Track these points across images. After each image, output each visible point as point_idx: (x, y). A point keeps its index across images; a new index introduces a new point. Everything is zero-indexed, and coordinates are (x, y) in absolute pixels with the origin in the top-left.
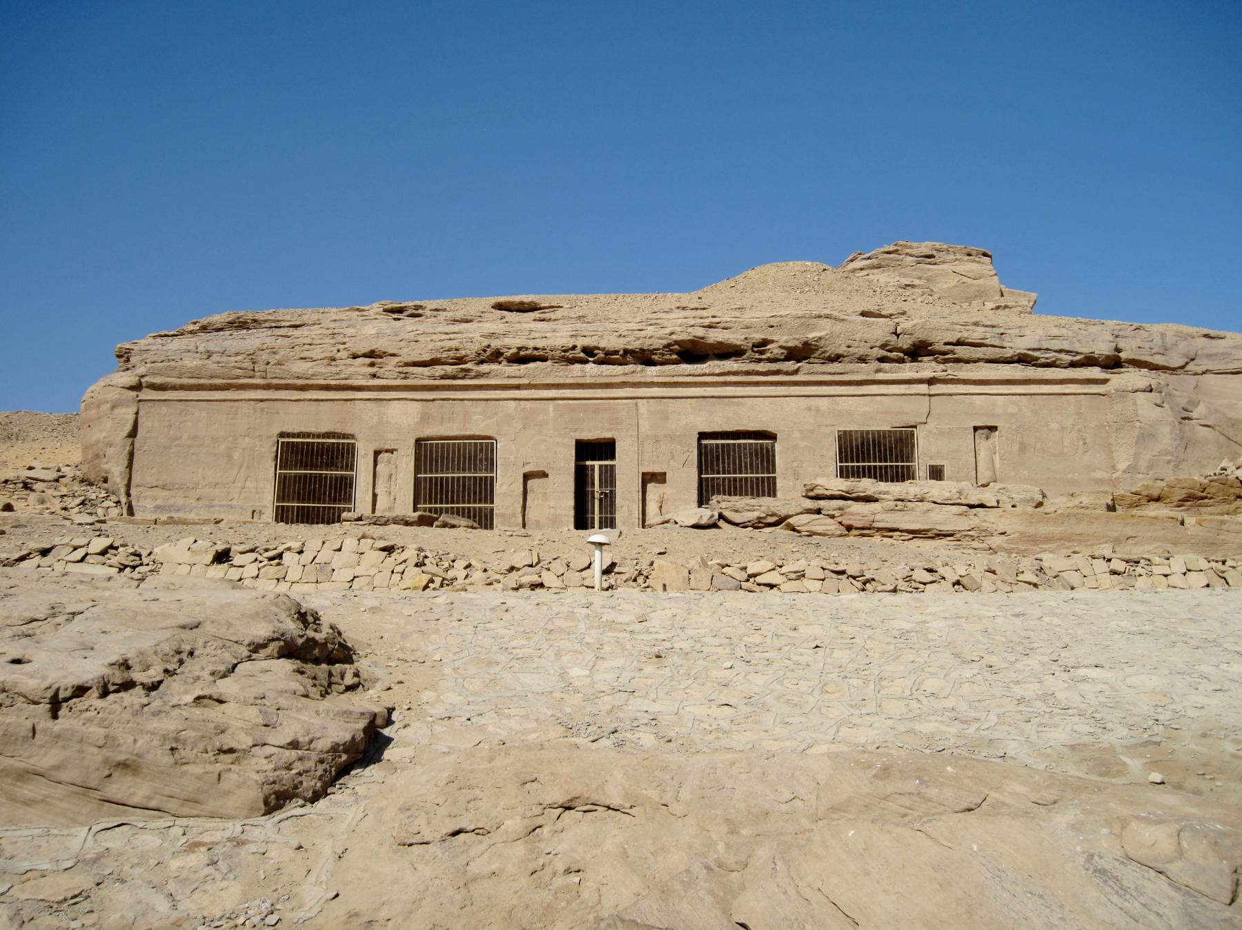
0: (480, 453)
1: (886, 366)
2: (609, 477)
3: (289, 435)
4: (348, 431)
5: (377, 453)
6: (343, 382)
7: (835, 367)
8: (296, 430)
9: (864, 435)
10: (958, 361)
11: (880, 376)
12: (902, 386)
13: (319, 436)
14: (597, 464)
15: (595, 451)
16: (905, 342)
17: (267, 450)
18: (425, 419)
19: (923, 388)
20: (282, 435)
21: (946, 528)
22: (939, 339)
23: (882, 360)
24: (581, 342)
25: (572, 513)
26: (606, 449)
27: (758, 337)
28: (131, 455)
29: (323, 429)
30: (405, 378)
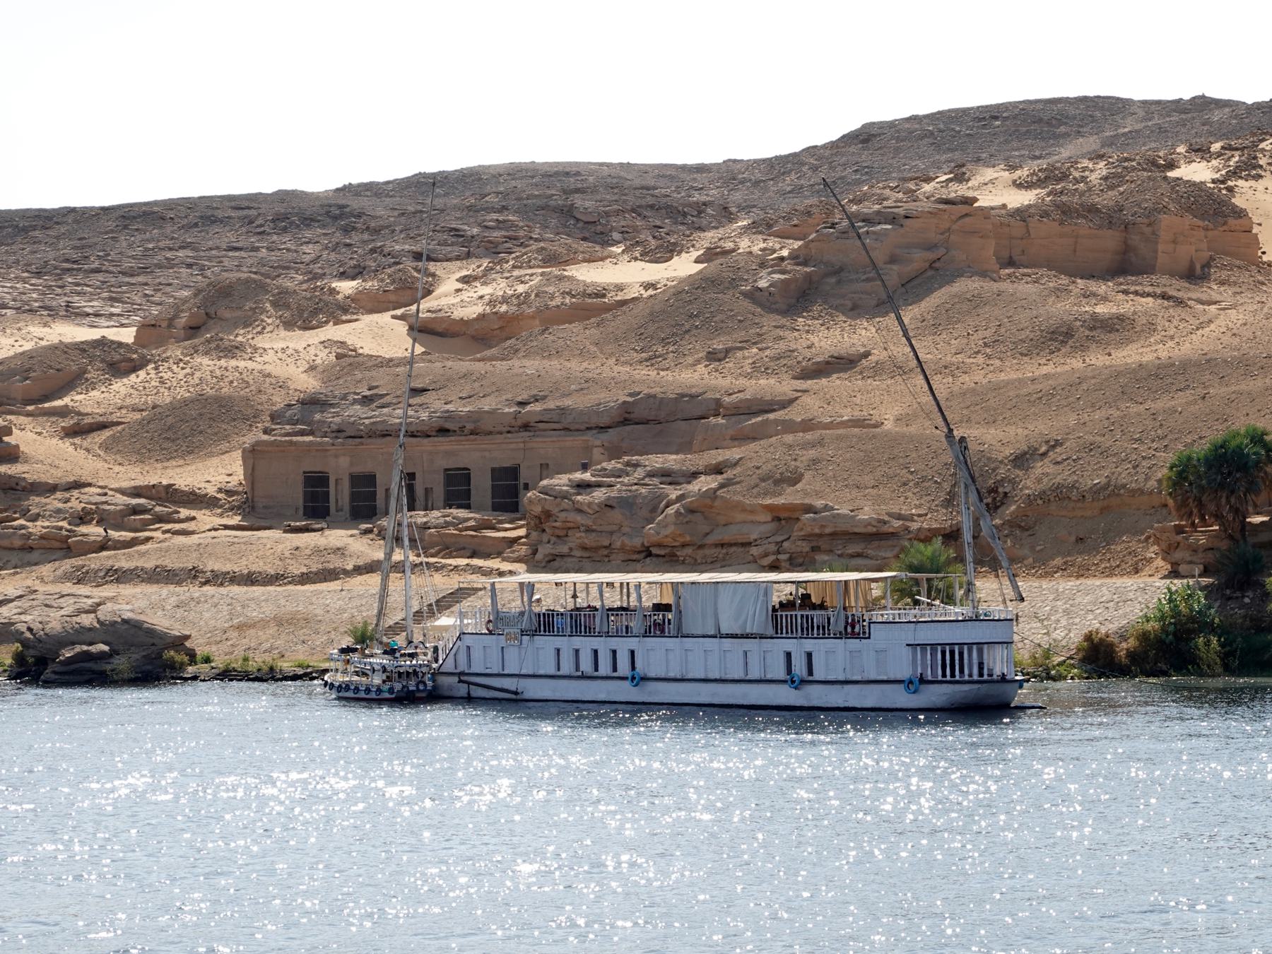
0: (370, 479)
16: (519, 423)
17: (301, 479)
19: (522, 445)
22: (533, 419)
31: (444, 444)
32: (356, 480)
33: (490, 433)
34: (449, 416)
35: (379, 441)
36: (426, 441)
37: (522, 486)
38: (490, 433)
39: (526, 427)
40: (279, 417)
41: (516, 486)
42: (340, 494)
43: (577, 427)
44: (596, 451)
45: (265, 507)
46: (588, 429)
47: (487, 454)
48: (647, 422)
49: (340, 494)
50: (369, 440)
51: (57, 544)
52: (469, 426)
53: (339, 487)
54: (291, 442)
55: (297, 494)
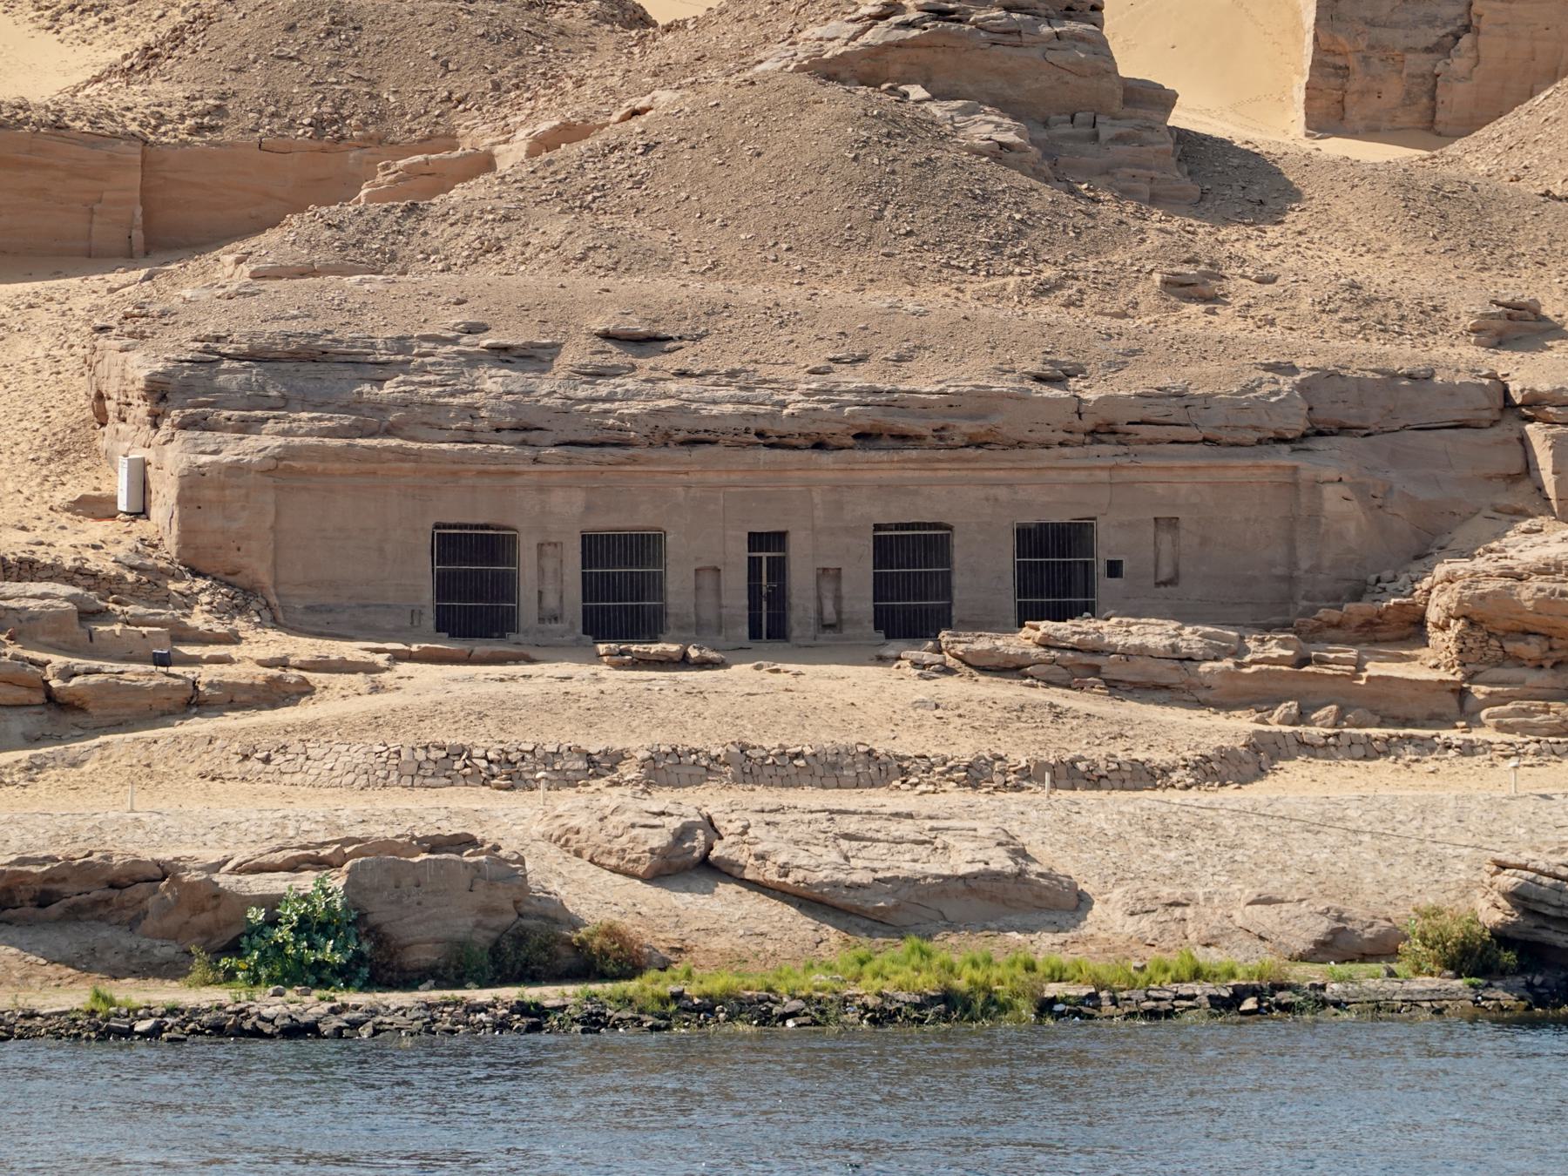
1: (1066, 451)
2: (779, 569)
3: (445, 526)
4: (506, 523)
5: (540, 546)
6: (503, 467)
7: (1018, 453)
8: (453, 520)
9: (1043, 527)
10: (1142, 441)
11: (1062, 463)
12: (1083, 473)
13: (477, 527)
14: (764, 555)
15: (768, 545)
16: (1088, 423)
17: (425, 541)
18: (589, 508)
19: (1103, 476)
20: (437, 526)
21: (1164, 681)
22: (1121, 417)
23: (1061, 444)
24: (754, 426)
25: (746, 613)
26: (777, 540)
27: (940, 423)
28: (276, 549)
29: (481, 521)
30: (570, 463)
31: (880, 466)
32: (595, 547)
33: (1020, 444)
34: (894, 403)
35: (683, 454)
36: (826, 458)
37: (1101, 568)
38: (1020, 444)
39: (1104, 432)
40: (187, 387)
41: (1088, 567)
42: (548, 577)
43: (1239, 436)
44: (1330, 492)
45: (310, 609)
46: (1259, 442)
47: (1003, 493)
48: (1343, 430)
49: (548, 577)
50: (655, 454)
51: (22, 694)
52: (967, 427)
53: (550, 564)
54: (404, 454)
55: (418, 579)
